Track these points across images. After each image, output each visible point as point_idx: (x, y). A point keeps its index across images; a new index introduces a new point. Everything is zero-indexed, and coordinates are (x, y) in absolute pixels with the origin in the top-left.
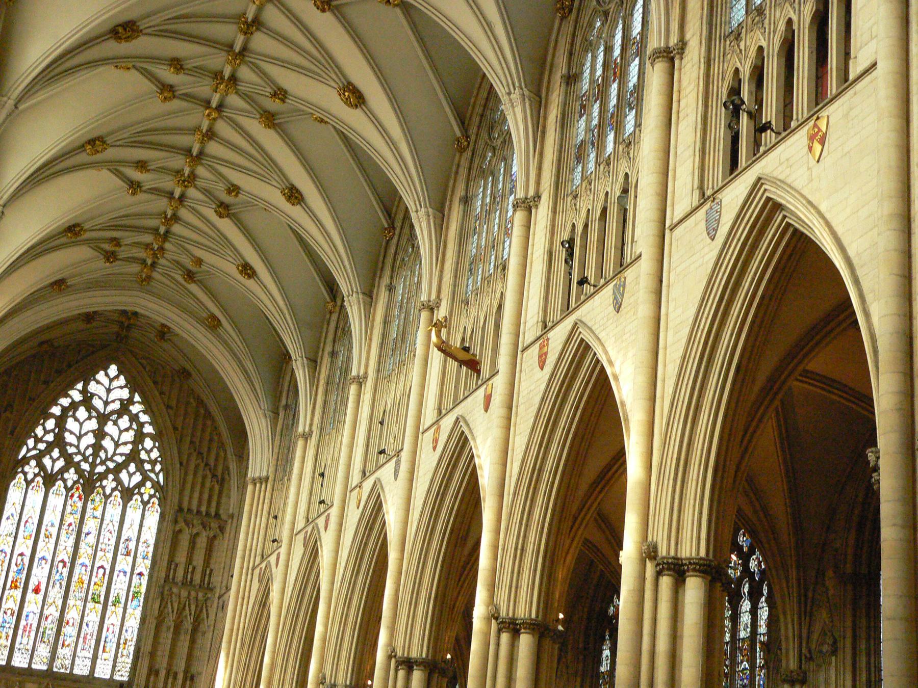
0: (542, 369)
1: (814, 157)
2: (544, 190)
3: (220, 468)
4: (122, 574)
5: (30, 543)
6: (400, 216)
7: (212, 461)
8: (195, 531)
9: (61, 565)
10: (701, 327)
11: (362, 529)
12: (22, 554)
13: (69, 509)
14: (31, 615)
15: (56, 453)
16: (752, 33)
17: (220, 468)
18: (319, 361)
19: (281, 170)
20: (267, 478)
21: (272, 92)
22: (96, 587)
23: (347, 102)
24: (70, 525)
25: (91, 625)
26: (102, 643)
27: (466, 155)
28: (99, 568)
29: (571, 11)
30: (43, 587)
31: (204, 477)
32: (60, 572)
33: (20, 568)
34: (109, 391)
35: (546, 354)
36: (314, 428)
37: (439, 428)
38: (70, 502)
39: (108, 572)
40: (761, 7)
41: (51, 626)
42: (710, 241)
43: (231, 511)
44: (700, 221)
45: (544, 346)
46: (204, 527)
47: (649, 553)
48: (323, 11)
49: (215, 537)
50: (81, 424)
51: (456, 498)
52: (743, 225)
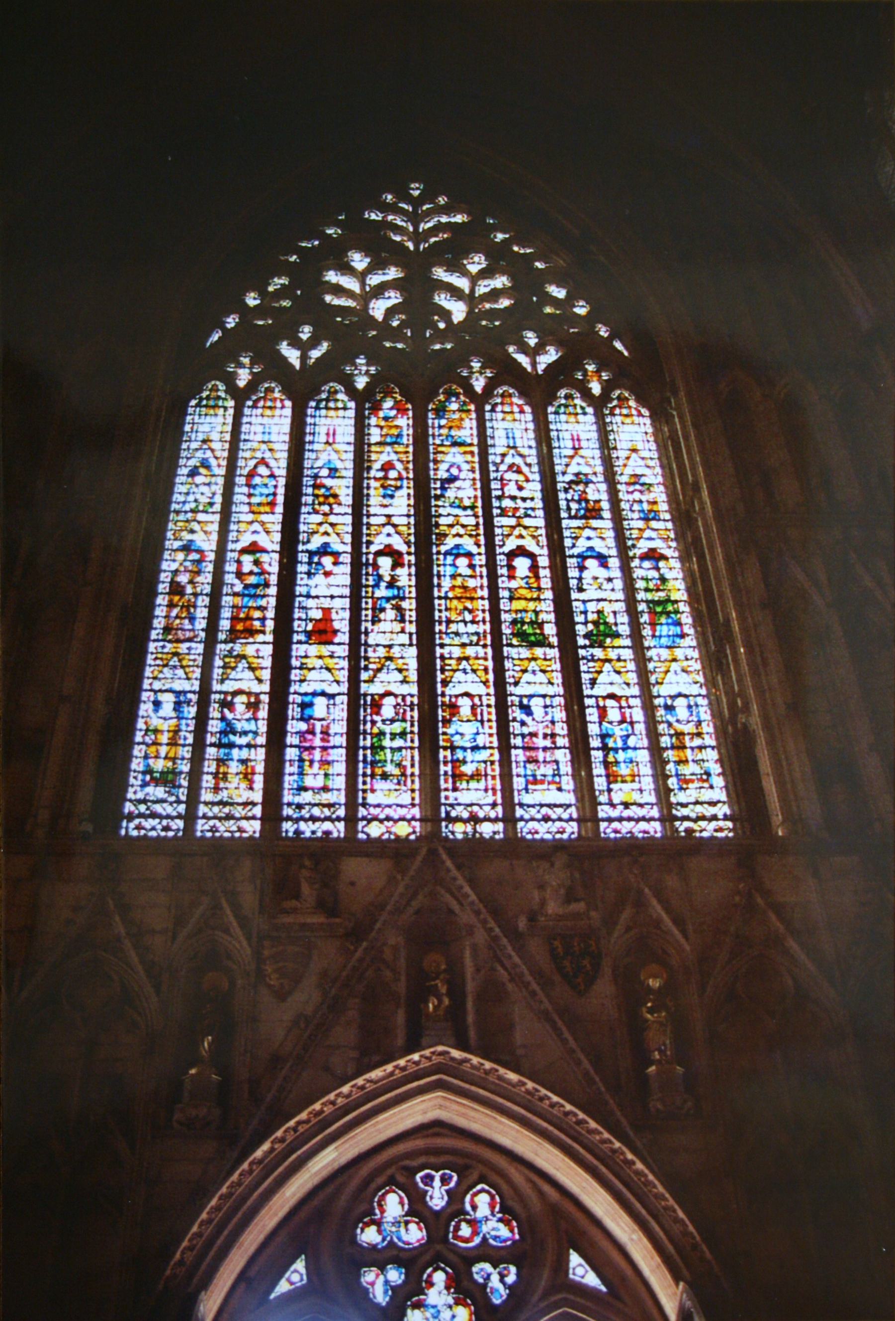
4: (591, 563)
5: (275, 520)
9: (385, 563)
12: (253, 549)
13: (375, 435)
14: (320, 702)
15: (305, 333)
22: (518, 605)
24: (387, 467)
25: (536, 705)
26: (597, 756)
28: (512, 555)
30: (342, 623)
32: (387, 578)
33: (252, 580)
34: (415, 218)
38: (373, 421)
39: (544, 561)
41: (397, 727)
50: (362, 277)
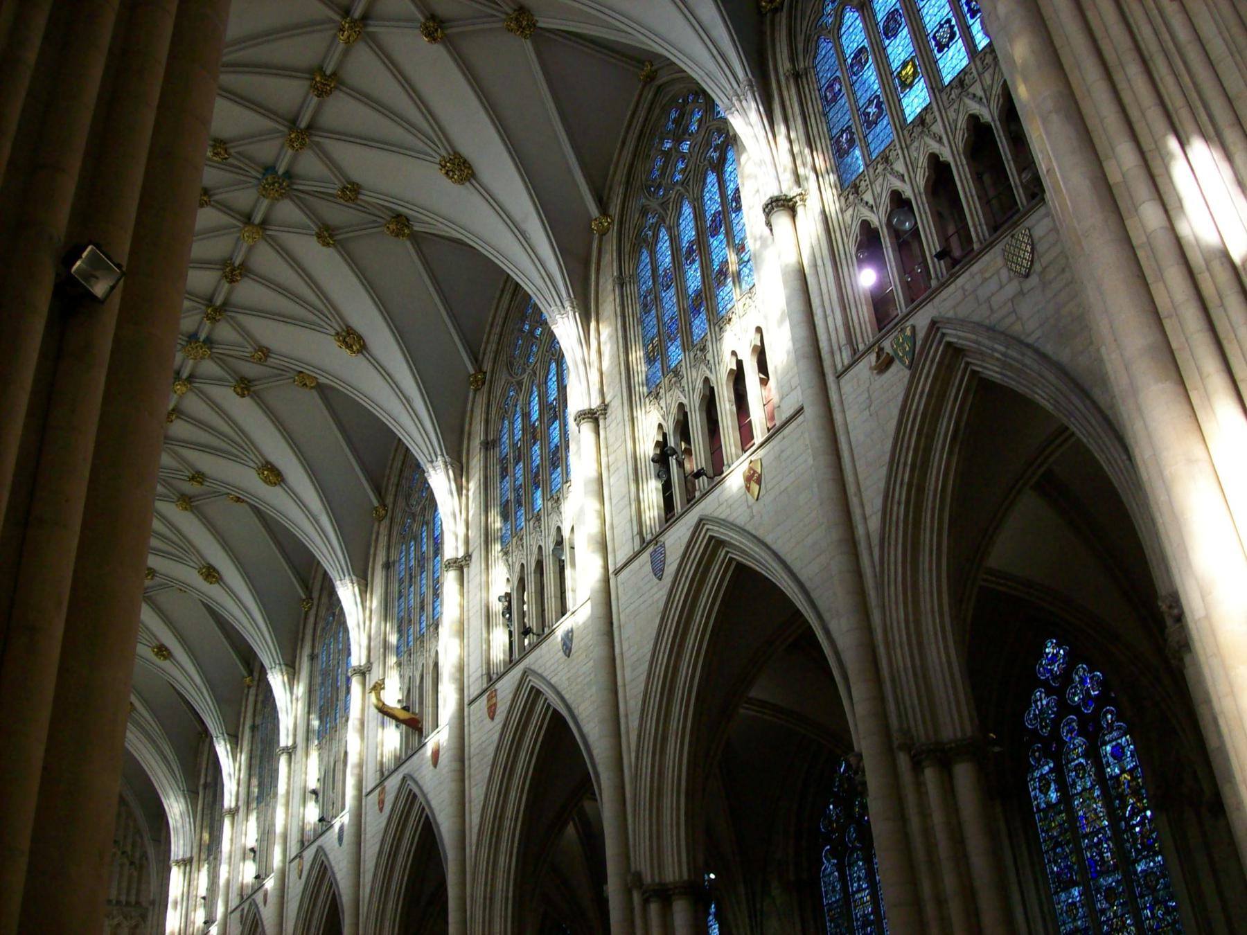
0: (492, 718)
1: (753, 497)
2: (474, 550)
3: (138, 855)
6: (317, 586)
7: (129, 849)
8: (116, 921)
10: (659, 662)
11: (306, 900)
16: (671, 392)
17: (138, 855)
18: (240, 736)
19: (198, 551)
20: (191, 860)
21: (191, 475)
23: (266, 481)
27: (383, 523)
29: (484, 383)
31: (122, 865)
35: (495, 704)
36: (240, 803)
37: (384, 788)
40: (677, 369)
42: (658, 581)
43: (151, 898)
44: (645, 563)
45: (492, 697)
46: (125, 918)
47: (633, 881)
48: (243, 396)
49: (137, 926)
51: (408, 856)
52: (690, 563)
